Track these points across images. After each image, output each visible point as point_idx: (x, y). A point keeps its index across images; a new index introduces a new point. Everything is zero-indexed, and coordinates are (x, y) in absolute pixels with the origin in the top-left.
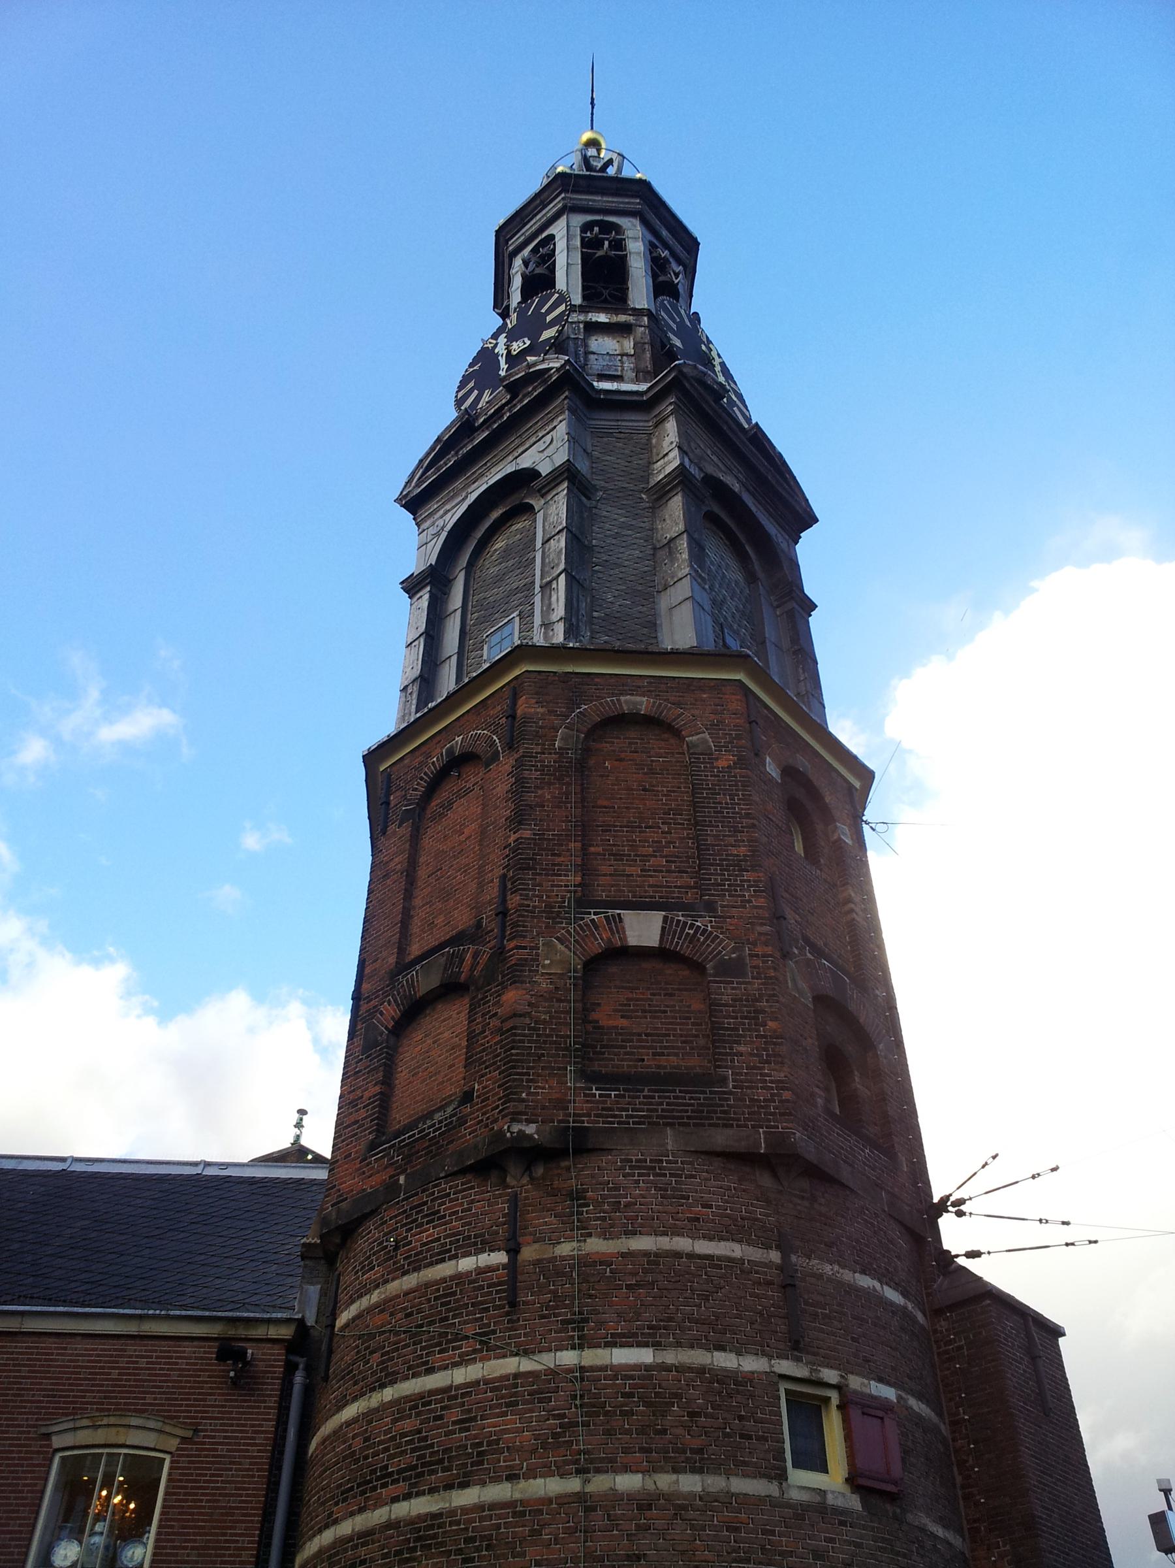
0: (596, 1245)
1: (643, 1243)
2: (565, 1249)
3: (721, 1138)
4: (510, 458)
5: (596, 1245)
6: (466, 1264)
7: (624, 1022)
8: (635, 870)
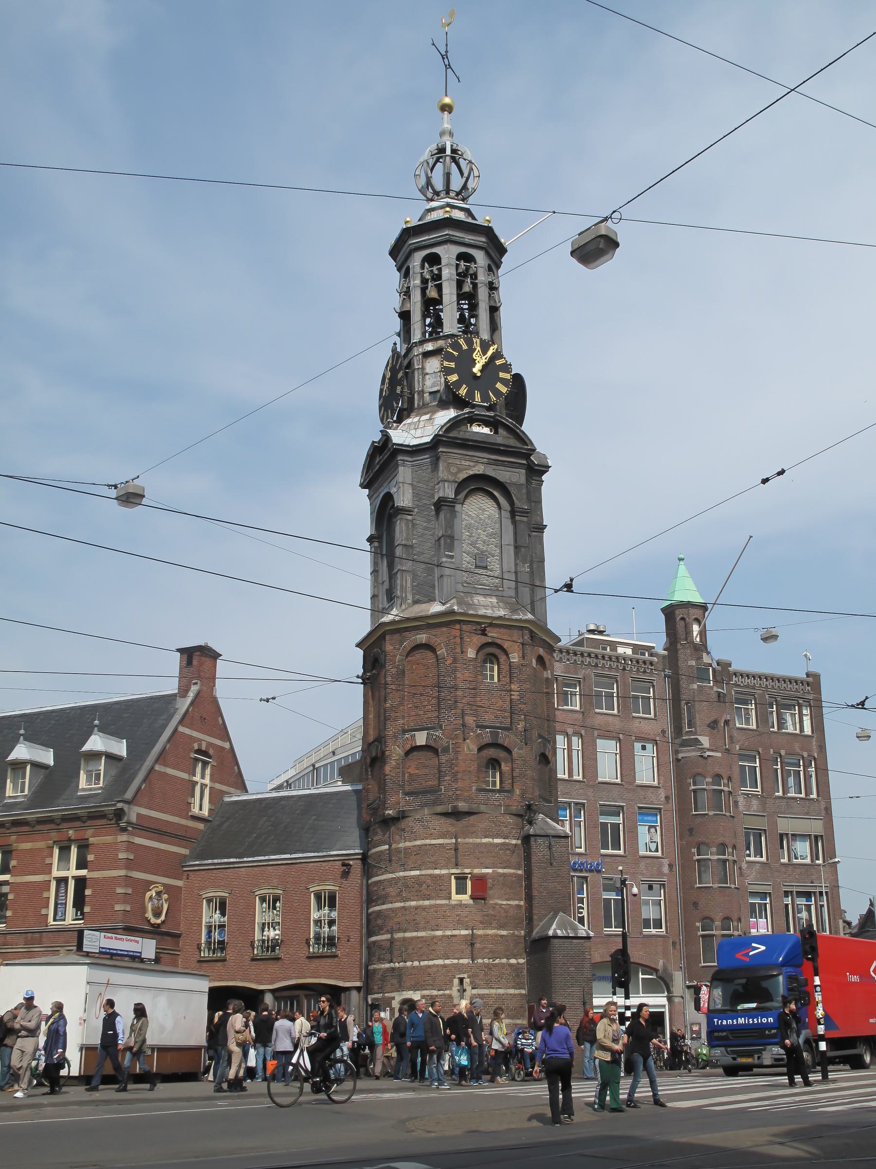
0: (408, 844)
1: (418, 843)
3: (440, 809)
5: (408, 844)
7: (417, 771)
8: (421, 713)
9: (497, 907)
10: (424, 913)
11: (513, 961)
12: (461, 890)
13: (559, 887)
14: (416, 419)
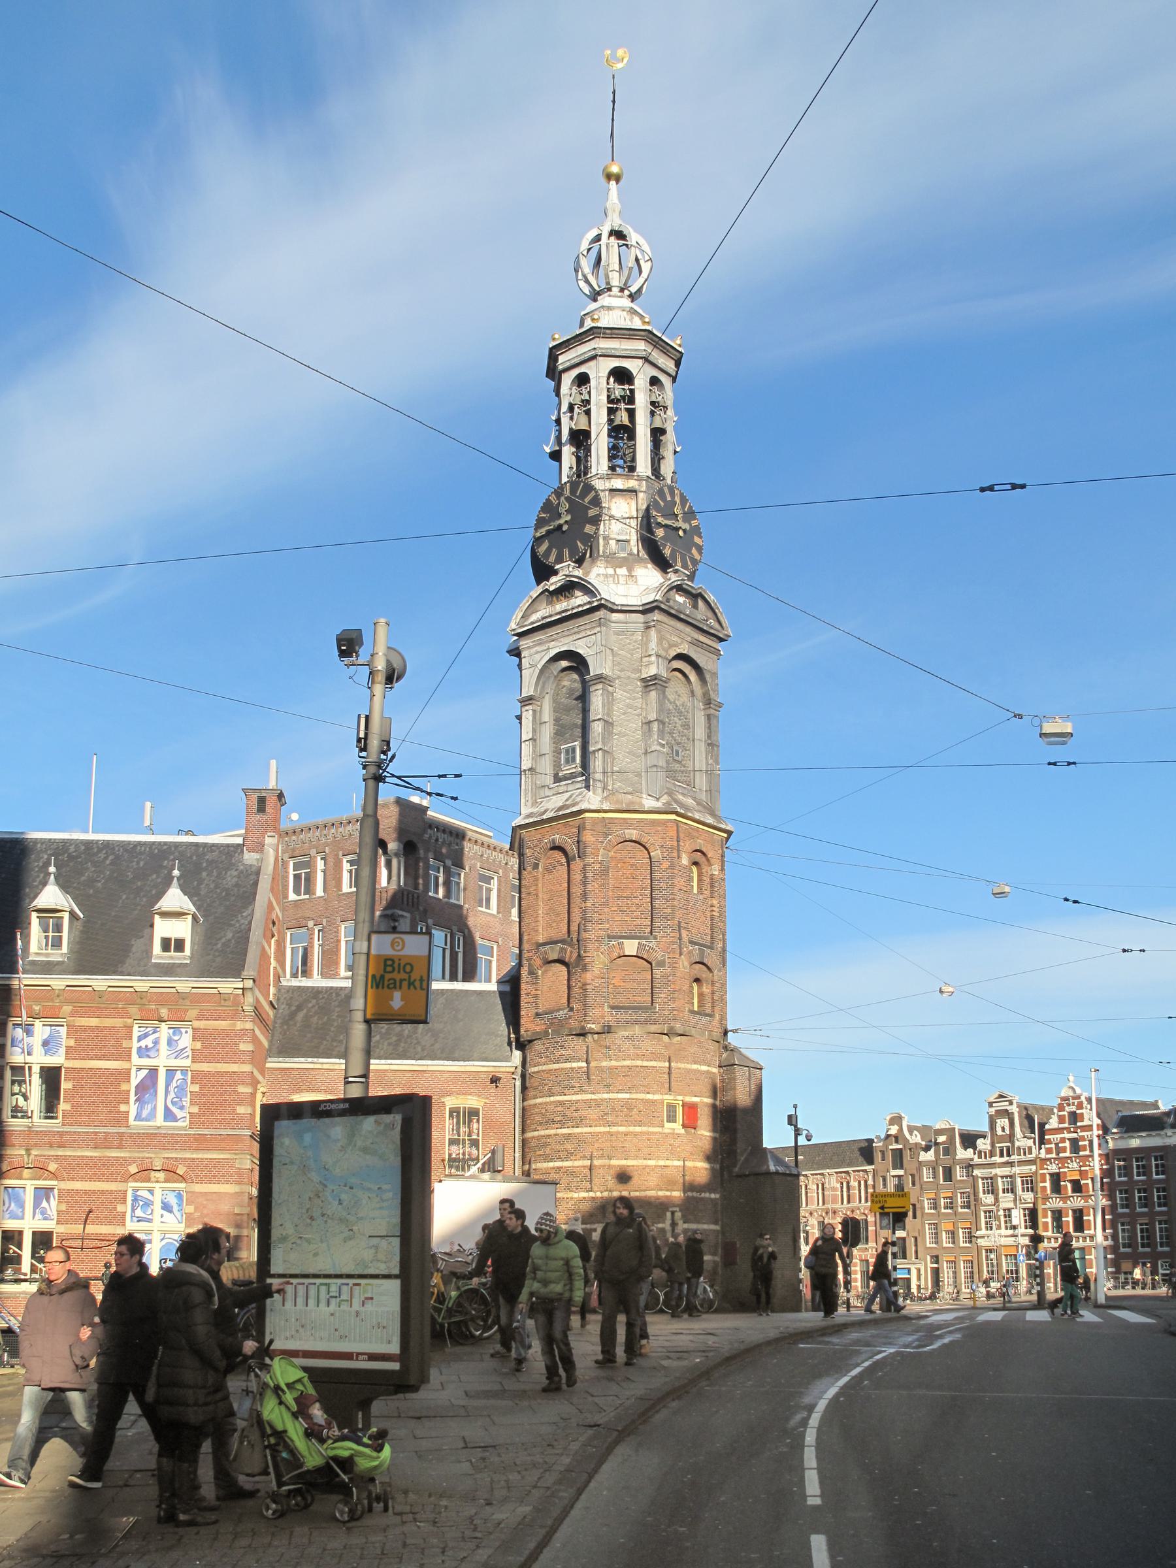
0: (613, 1063)
2: (604, 1064)
3: (653, 1028)
4: (571, 638)
5: (613, 1063)
6: (574, 1065)
10: (635, 1141)
11: (713, 1196)
12: (672, 1119)
14: (610, 571)
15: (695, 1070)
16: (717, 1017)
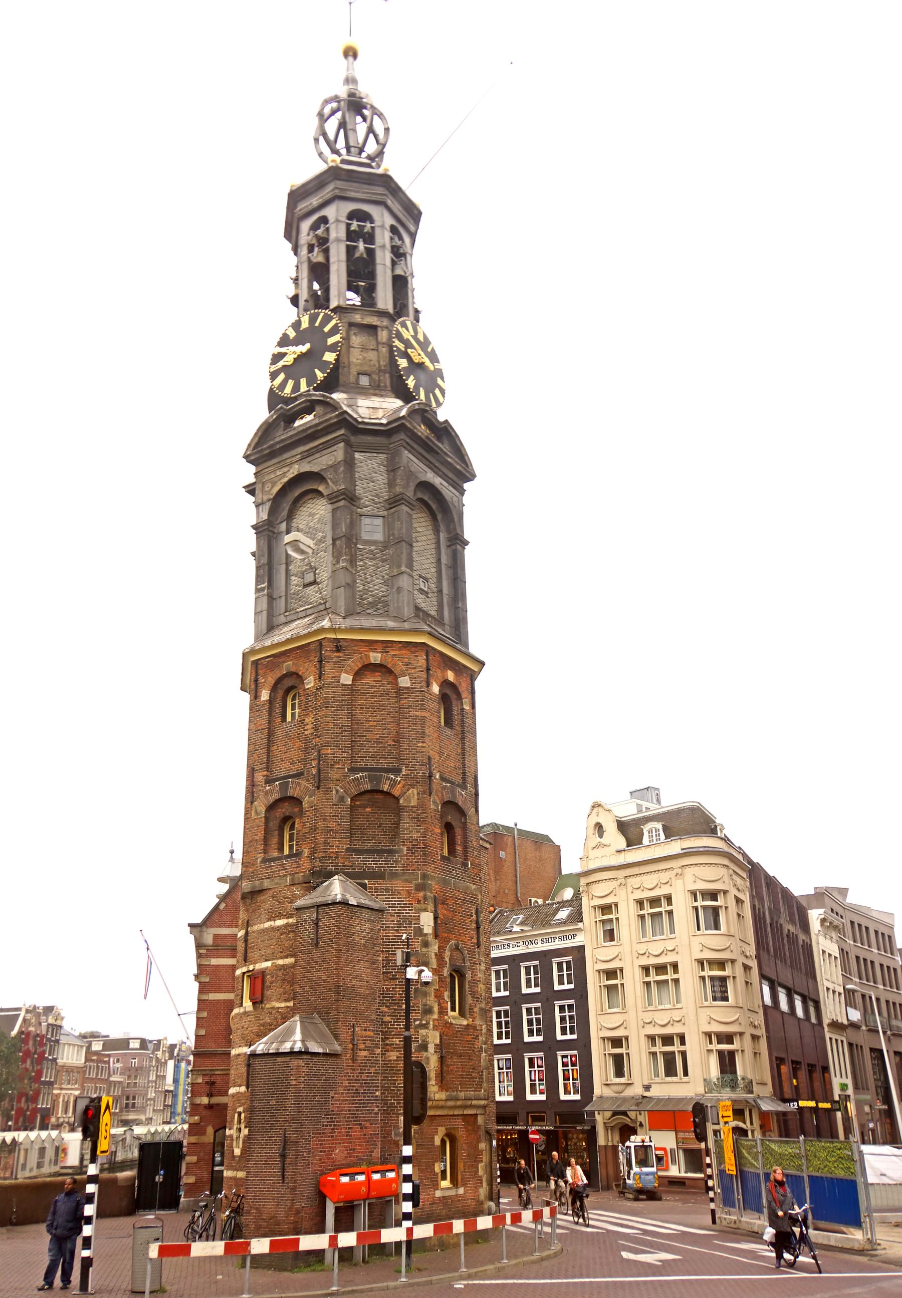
9: (274, 1012)
13: (324, 977)
15: (267, 930)
16: (306, 852)
